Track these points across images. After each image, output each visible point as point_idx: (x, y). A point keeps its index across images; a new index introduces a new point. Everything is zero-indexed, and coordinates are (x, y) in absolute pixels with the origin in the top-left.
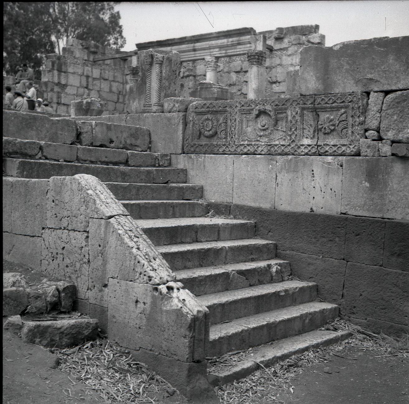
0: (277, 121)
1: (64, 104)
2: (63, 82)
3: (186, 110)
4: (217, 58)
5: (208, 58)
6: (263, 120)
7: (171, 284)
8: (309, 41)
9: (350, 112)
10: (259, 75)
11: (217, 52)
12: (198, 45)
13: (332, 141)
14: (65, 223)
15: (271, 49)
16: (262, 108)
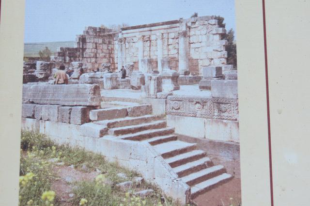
0: (203, 106)
1: (85, 57)
2: (84, 47)
3: (166, 98)
4: (163, 34)
5: (158, 34)
6: (198, 105)
7: (177, 179)
8: (209, 24)
9: (232, 105)
10: (185, 42)
11: (162, 31)
12: (152, 28)
13: (226, 114)
14: (138, 158)
15: (190, 28)
16: (198, 101)
